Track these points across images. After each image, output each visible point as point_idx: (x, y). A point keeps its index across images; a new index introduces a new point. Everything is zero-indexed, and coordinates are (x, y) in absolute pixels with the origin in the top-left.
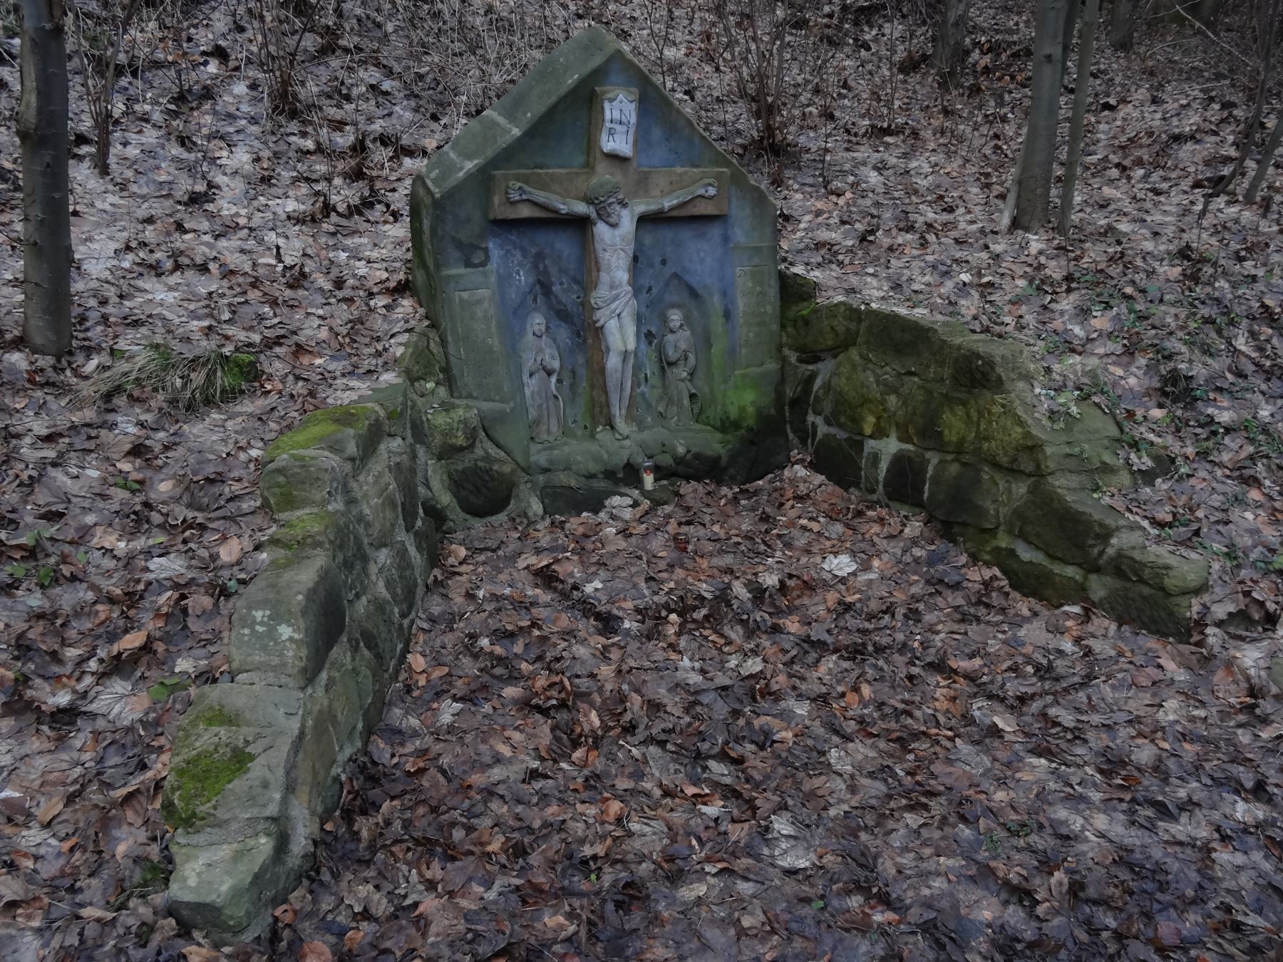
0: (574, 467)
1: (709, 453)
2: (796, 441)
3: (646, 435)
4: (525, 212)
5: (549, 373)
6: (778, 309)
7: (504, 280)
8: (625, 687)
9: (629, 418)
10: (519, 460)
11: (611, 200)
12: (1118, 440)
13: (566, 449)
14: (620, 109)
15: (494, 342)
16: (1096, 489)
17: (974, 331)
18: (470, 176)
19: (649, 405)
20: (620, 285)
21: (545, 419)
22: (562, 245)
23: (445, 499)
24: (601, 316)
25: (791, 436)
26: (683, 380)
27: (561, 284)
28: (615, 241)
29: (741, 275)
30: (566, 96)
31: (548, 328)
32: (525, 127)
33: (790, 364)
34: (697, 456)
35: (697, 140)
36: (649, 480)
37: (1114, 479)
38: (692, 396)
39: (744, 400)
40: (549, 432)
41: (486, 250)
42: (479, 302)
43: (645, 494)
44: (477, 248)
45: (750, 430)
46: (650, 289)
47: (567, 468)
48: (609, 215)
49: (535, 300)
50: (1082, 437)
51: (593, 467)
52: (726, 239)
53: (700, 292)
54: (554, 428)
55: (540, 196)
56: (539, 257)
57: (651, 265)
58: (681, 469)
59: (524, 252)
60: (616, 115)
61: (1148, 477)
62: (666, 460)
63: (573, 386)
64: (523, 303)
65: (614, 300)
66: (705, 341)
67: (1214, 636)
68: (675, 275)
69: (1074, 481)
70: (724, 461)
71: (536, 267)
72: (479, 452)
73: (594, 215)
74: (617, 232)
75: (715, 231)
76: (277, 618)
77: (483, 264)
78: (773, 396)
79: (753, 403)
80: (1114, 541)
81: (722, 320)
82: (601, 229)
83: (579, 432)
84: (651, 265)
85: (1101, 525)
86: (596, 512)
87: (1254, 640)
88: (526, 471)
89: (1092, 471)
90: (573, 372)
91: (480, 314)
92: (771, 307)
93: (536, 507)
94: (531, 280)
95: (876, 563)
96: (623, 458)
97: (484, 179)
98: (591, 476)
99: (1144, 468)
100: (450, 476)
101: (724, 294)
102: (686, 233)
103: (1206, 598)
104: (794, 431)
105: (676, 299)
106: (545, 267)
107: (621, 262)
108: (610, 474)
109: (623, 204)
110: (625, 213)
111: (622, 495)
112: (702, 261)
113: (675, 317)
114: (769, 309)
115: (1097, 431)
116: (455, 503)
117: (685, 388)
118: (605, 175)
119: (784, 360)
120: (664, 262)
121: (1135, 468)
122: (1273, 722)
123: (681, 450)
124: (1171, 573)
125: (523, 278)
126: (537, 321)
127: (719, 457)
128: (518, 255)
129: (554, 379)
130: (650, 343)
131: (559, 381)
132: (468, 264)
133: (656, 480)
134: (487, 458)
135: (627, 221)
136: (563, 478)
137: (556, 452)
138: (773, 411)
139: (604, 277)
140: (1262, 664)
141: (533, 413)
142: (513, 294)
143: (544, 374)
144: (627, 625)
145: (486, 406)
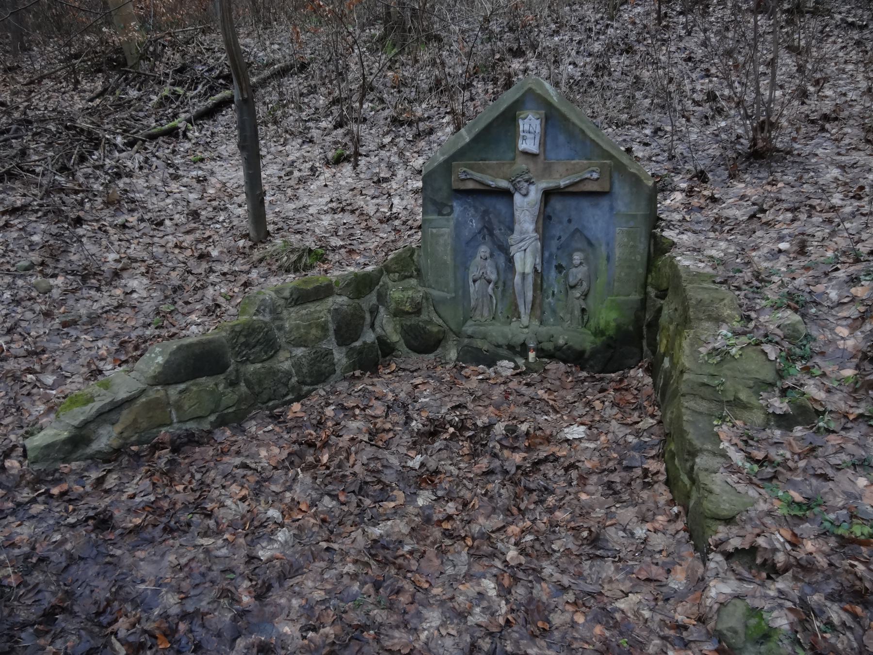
0: (489, 339)
1: (577, 347)
2: (649, 352)
3: (543, 329)
4: (471, 185)
5: (489, 282)
7: (458, 226)
8: (353, 449)
9: (531, 316)
10: (453, 327)
12: (772, 385)
13: (490, 328)
14: (530, 125)
15: (448, 258)
16: (722, 419)
17: (714, 282)
18: (440, 165)
19: (554, 312)
20: (527, 232)
21: (479, 308)
22: (500, 205)
23: (395, 338)
24: (513, 250)
25: (645, 348)
26: (578, 298)
28: (526, 206)
29: (620, 234)
30: (497, 118)
31: (492, 255)
32: (472, 135)
34: (569, 348)
35: (588, 142)
36: (532, 355)
37: (746, 414)
38: (583, 310)
39: (607, 317)
40: (482, 316)
41: (452, 207)
42: (442, 235)
43: (527, 364)
44: (446, 205)
45: (610, 338)
46: (560, 238)
47: (484, 338)
49: (484, 238)
50: (729, 373)
51: (501, 341)
52: (612, 208)
53: (593, 242)
54: (486, 314)
55: (478, 176)
56: (486, 212)
57: (561, 222)
58: (558, 354)
60: (527, 127)
61: (785, 421)
62: (548, 346)
63: (504, 291)
64: (474, 238)
65: (522, 241)
66: (592, 276)
67: (716, 560)
68: (577, 230)
69: (703, 406)
70: (587, 355)
71: (483, 218)
72: (424, 317)
73: (512, 189)
74: (526, 199)
75: (605, 203)
76: (161, 353)
77: (449, 214)
78: (633, 317)
79: (615, 320)
80: (698, 460)
81: (605, 262)
82: (517, 198)
83: (503, 320)
84: (561, 222)
85: (691, 444)
86: (489, 367)
87: (741, 579)
88: (458, 334)
89: (722, 402)
90: (504, 283)
91: (441, 241)
92: (640, 258)
93: (453, 354)
94: (480, 226)
95: (603, 438)
96: (520, 339)
97: (447, 166)
98: (499, 346)
99: (778, 412)
100: (402, 326)
101: (608, 245)
102: (585, 203)
103: (735, 530)
104: (649, 345)
105: (579, 245)
108: (511, 347)
109: (530, 182)
110: (533, 188)
111: (510, 360)
112: (596, 222)
113: (577, 257)
114: (638, 257)
115: (747, 372)
116: (402, 341)
117: (579, 304)
118: (522, 164)
119: (646, 294)
120: (570, 221)
121: (771, 411)
122: (690, 649)
123: (561, 342)
124: (712, 497)
125: (475, 224)
126: (484, 250)
127: (582, 353)
128: (472, 211)
129: (491, 286)
130: (560, 272)
131: (496, 286)
132: (440, 213)
133: (537, 356)
134: (430, 322)
135: (535, 194)
136: (479, 343)
137: (482, 328)
138: (631, 328)
139: (517, 227)
140: (721, 599)
141: (473, 303)
142: (466, 234)
143: (483, 281)
144: (414, 423)
145: (435, 293)
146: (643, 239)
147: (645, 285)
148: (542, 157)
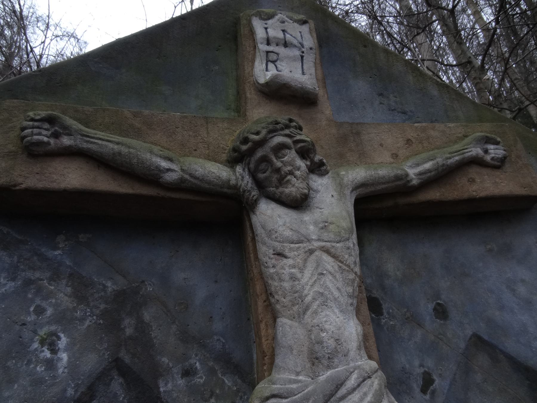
4: (72, 177)
11: (278, 139)
22: (191, 275)
27: (188, 373)
46: (427, 382)
48: (282, 181)
56: (127, 300)
57: (413, 320)
59: (82, 289)
68: (478, 342)
71: (110, 323)
74: (307, 217)
82: (269, 216)
84: (413, 320)
94: (91, 362)
102: (469, 248)
106: (142, 328)
107: (328, 280)
120: (441, 312)
128: (63, 296)
135: (332, 202)
139: (289, 330)
148: (326, 109)
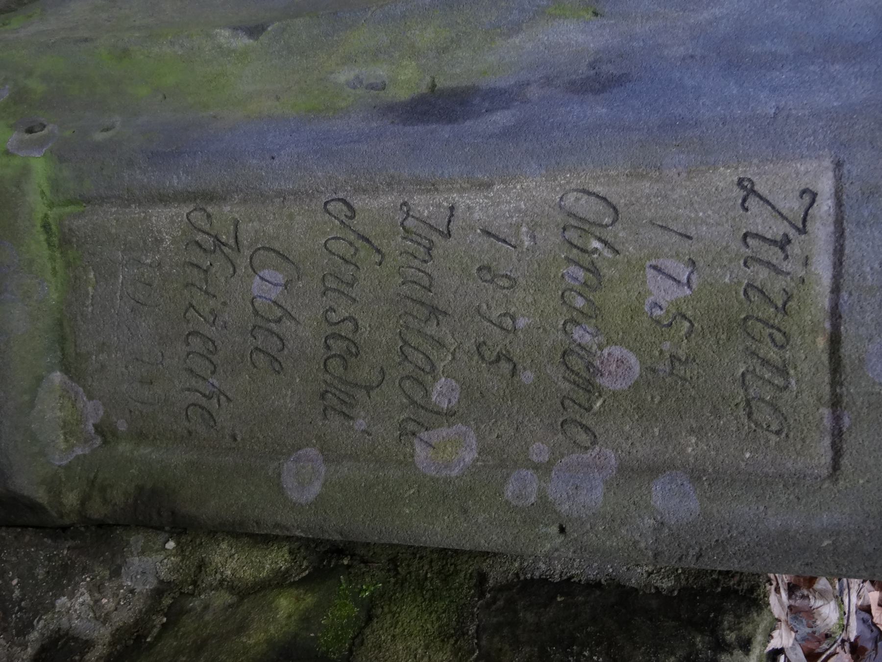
6: (439, 530)
33: (62, 578)
81: (407, 80)
101: (600, 81)
114: (449, 452)
146: (672, 502)
147: (157, 512)
